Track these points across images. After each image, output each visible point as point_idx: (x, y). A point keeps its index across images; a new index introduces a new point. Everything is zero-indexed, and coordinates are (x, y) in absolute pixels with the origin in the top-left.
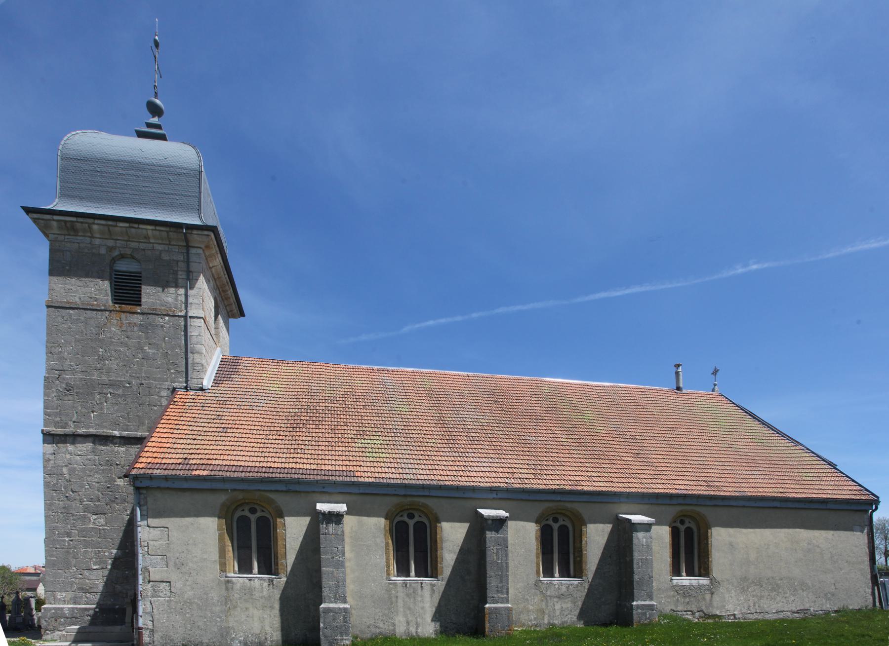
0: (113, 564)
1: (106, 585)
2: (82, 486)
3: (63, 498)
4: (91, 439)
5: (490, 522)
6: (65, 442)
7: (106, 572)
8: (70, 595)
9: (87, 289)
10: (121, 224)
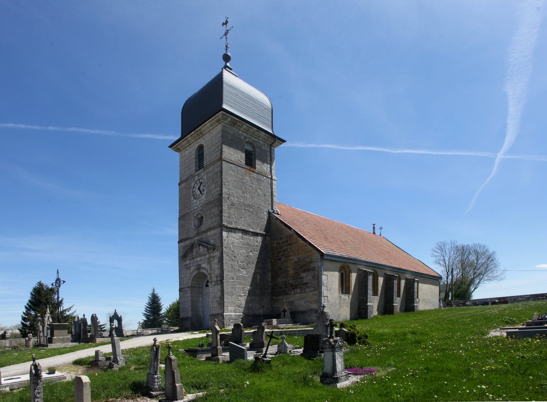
0: (248, 294)
1: (246, 304)
2: (238, 255)
3: (231, 260)
4: (241, 231)
5: (182, 293)
6: (231, 232)
7: (246, 297)
8: (233, 308)
9: (236, 155)
10: (255, 129)
